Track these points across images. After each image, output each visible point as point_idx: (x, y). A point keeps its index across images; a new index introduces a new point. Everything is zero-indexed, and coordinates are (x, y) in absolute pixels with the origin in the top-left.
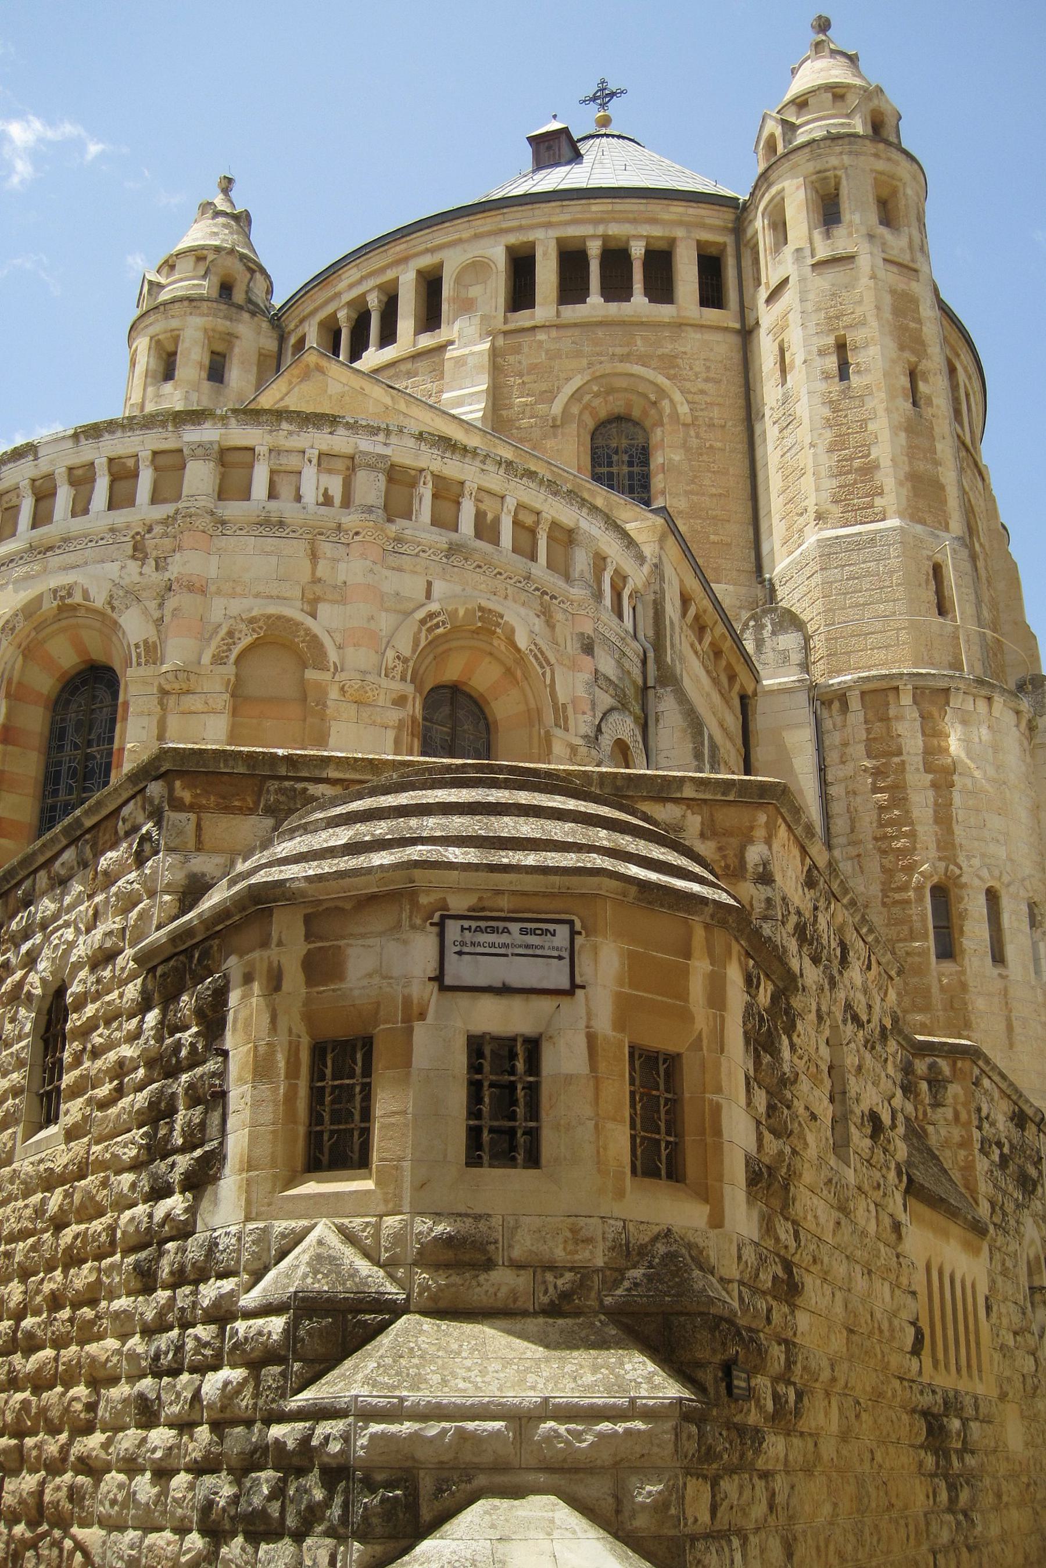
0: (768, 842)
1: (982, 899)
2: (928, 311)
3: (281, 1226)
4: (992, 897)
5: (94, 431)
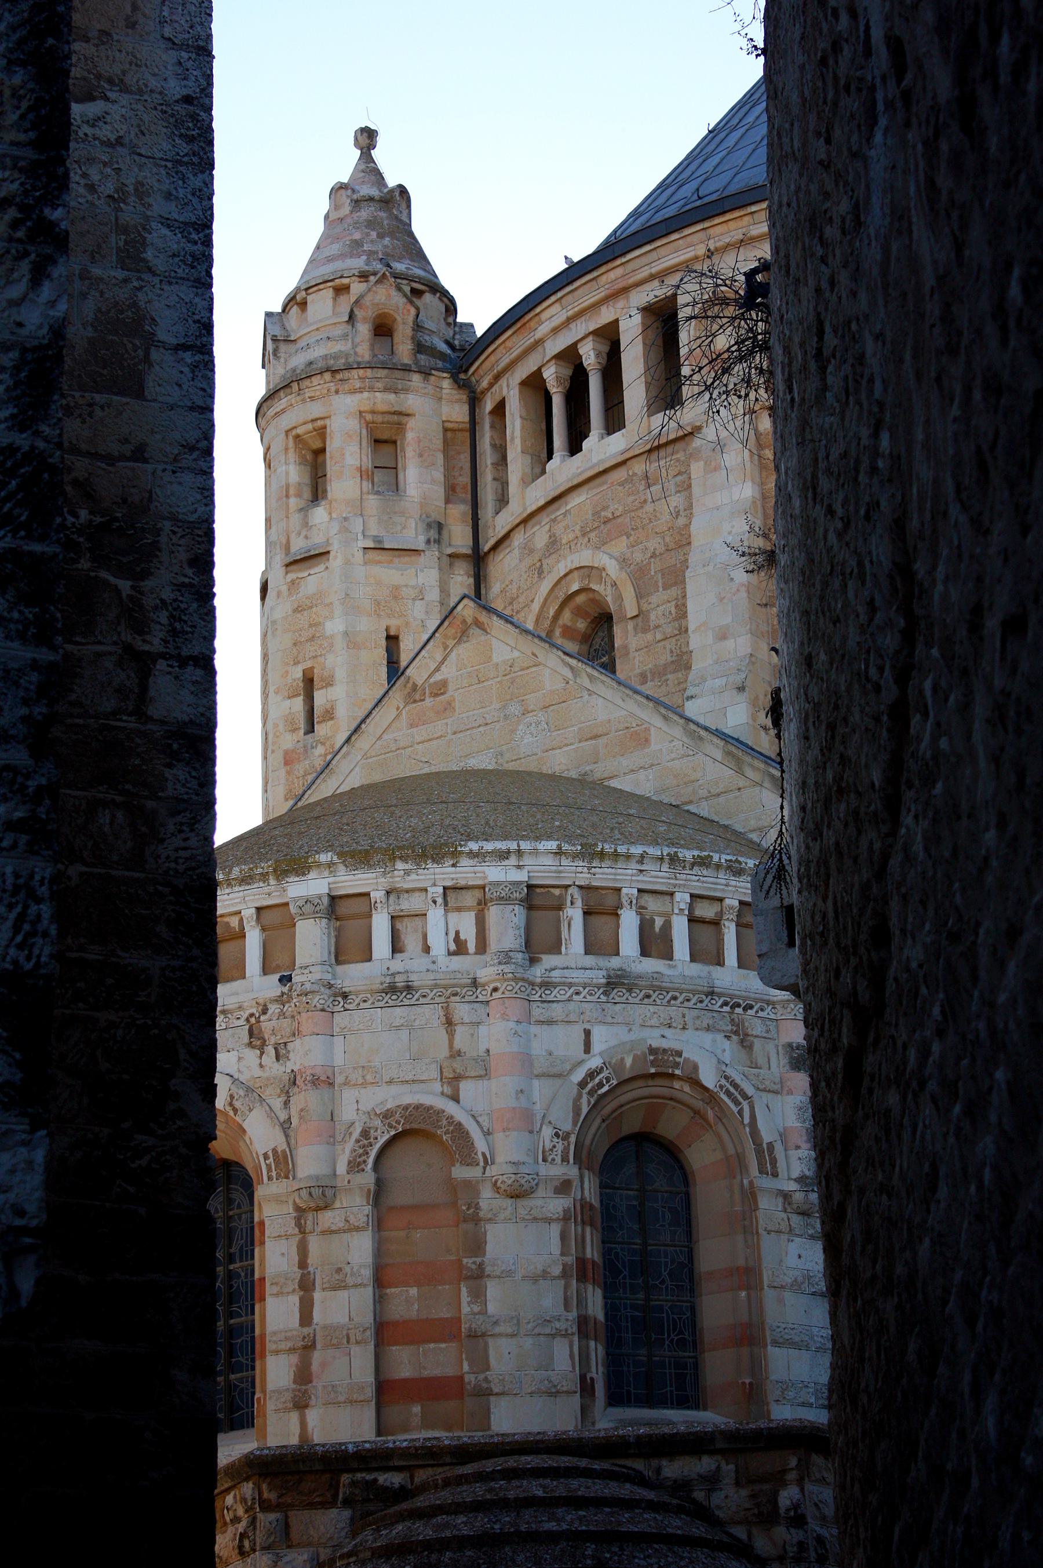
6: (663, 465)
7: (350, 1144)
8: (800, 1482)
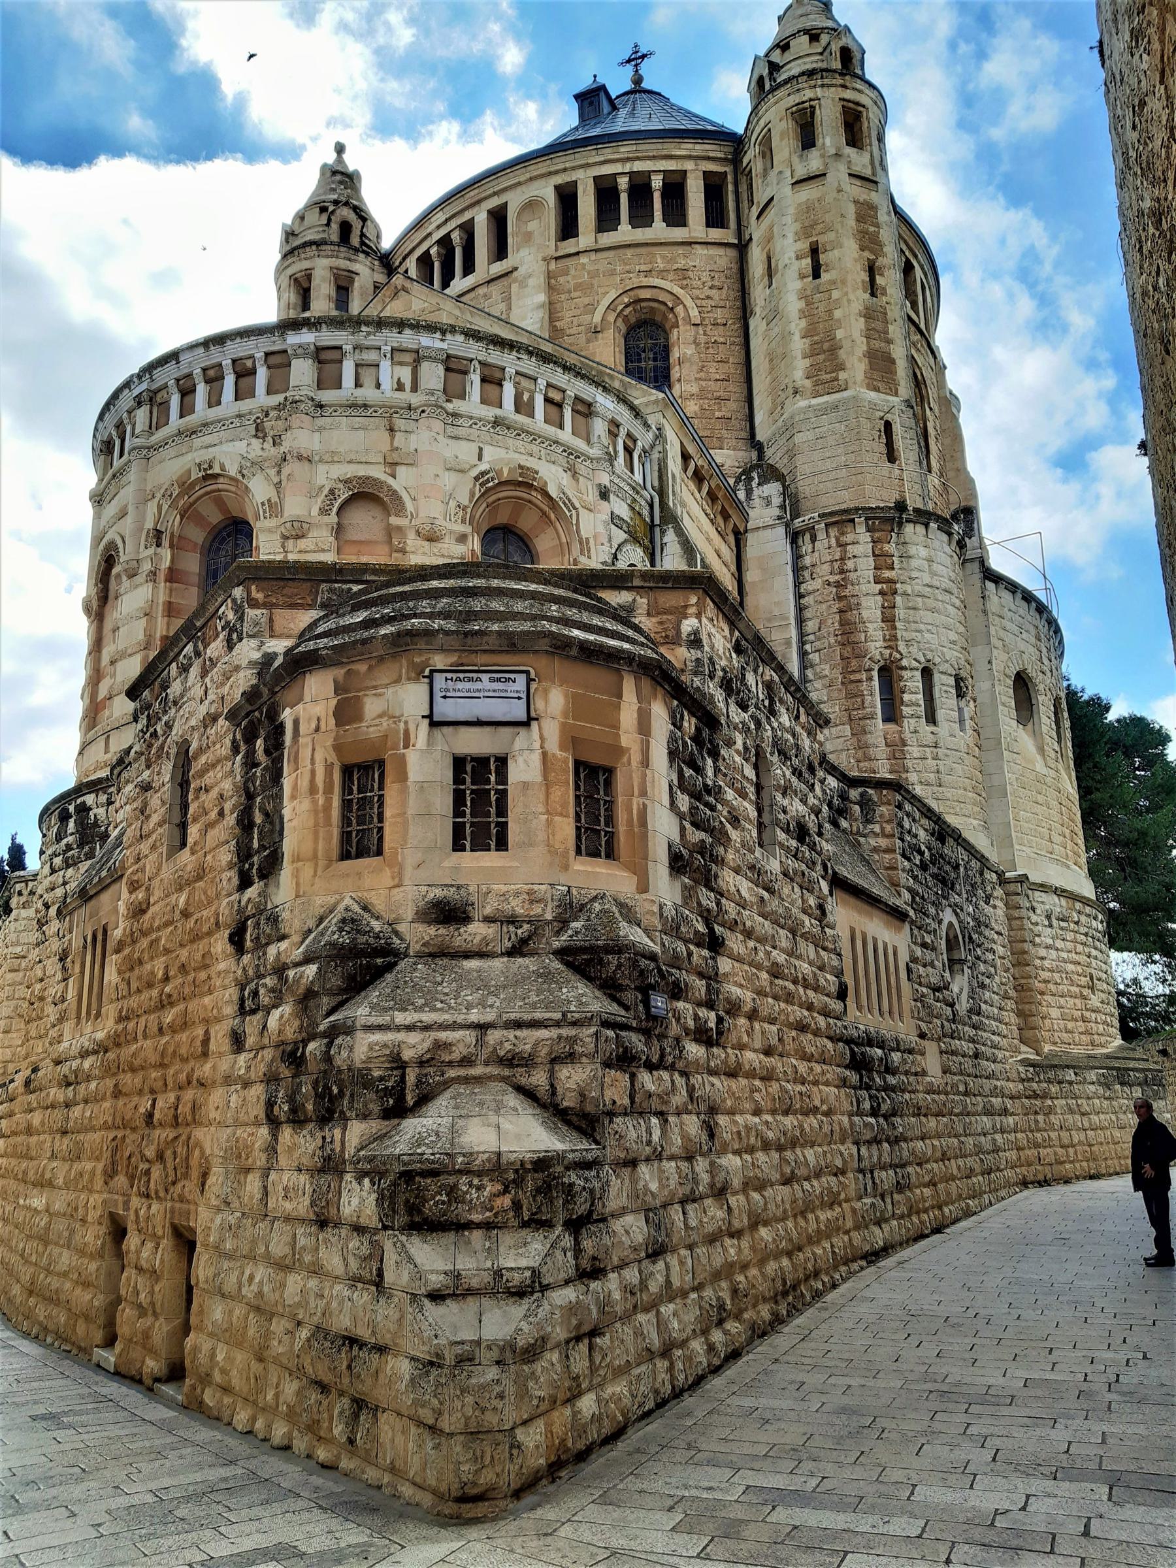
0: (698, 616)
1: (918, 675)
2: (884, 216)
3: (319, 901)
4: (927, 673)
5: (220, 340)
6: (495, 290)
7: (322, 497)
8: (698, 616)
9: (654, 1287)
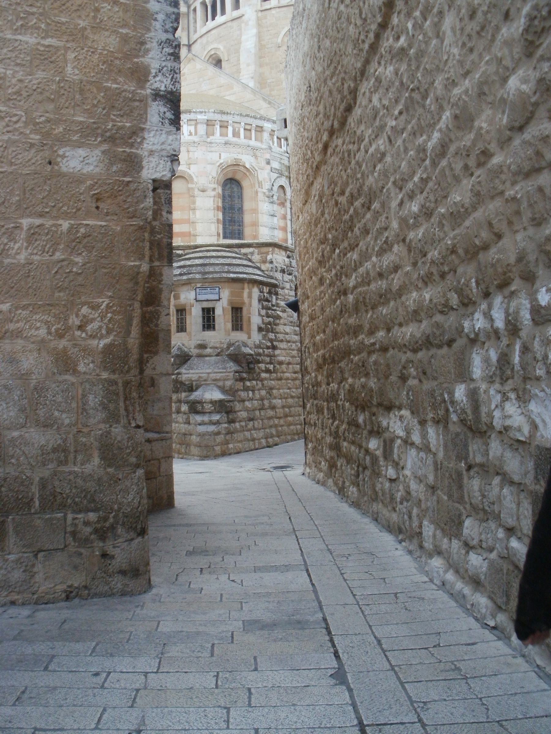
0: (272, 254)
6: (235, 23)
8: (272, 254)
9: (249, 427)
